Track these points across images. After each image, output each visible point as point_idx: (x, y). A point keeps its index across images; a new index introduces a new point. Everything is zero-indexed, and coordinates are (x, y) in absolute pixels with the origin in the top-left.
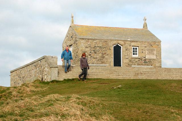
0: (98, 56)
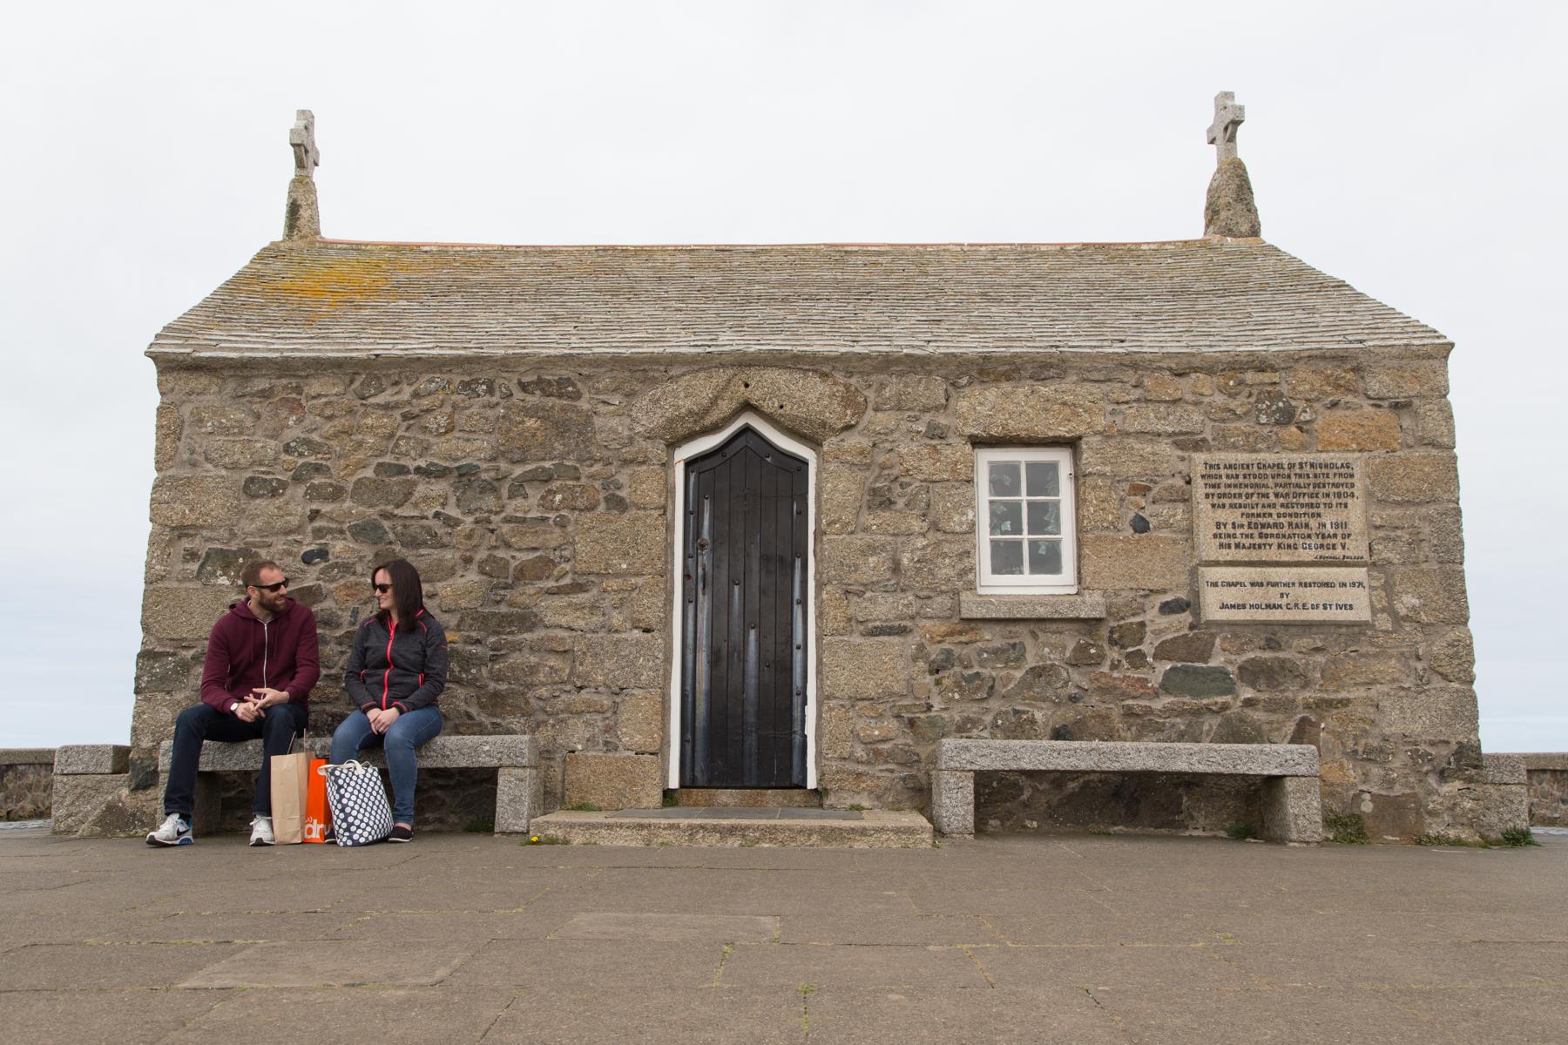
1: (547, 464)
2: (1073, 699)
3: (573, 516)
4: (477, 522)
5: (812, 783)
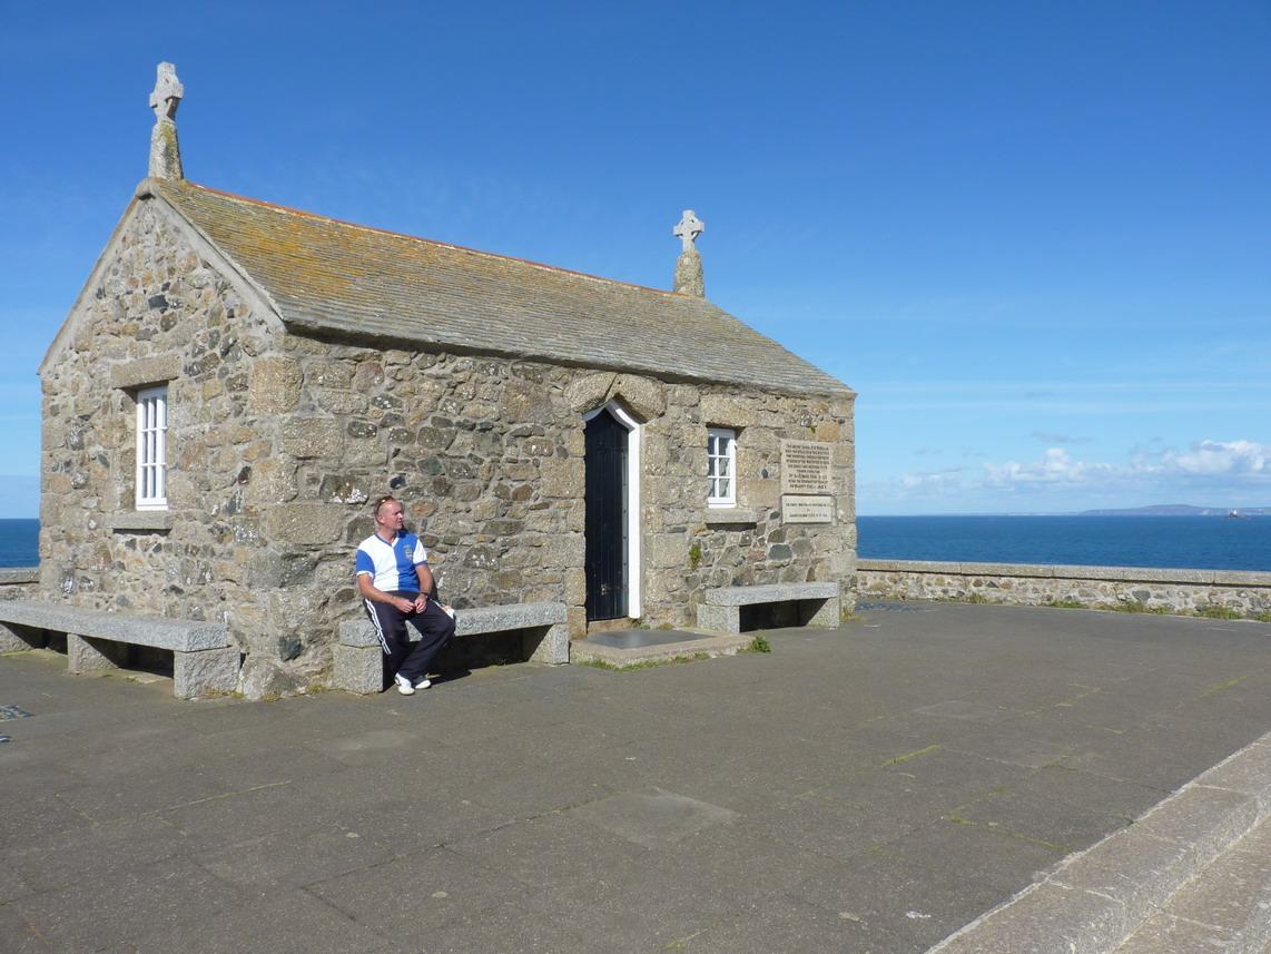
0: (463, 524)
1: (529, 425)
2: (740, 563)
3: (542, 459)
4: (493, 461)
5: (634, 610)
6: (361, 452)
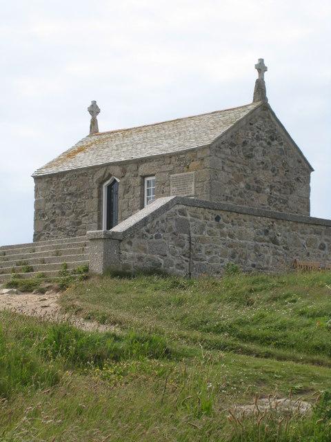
6: (49, 205)
